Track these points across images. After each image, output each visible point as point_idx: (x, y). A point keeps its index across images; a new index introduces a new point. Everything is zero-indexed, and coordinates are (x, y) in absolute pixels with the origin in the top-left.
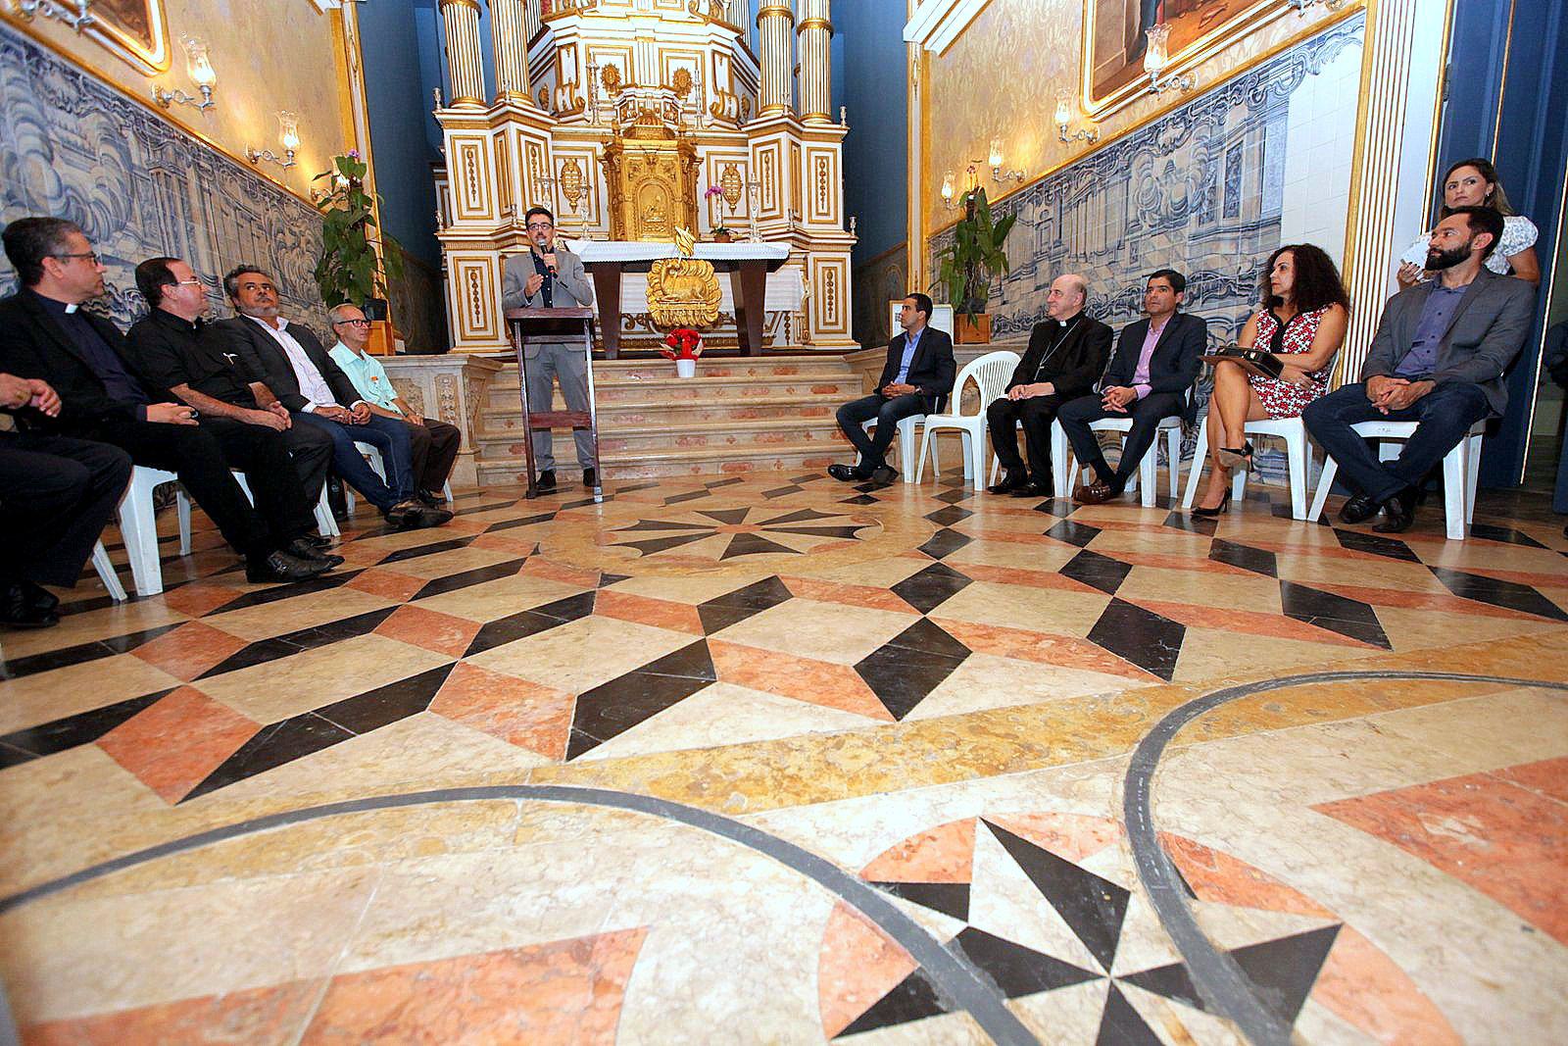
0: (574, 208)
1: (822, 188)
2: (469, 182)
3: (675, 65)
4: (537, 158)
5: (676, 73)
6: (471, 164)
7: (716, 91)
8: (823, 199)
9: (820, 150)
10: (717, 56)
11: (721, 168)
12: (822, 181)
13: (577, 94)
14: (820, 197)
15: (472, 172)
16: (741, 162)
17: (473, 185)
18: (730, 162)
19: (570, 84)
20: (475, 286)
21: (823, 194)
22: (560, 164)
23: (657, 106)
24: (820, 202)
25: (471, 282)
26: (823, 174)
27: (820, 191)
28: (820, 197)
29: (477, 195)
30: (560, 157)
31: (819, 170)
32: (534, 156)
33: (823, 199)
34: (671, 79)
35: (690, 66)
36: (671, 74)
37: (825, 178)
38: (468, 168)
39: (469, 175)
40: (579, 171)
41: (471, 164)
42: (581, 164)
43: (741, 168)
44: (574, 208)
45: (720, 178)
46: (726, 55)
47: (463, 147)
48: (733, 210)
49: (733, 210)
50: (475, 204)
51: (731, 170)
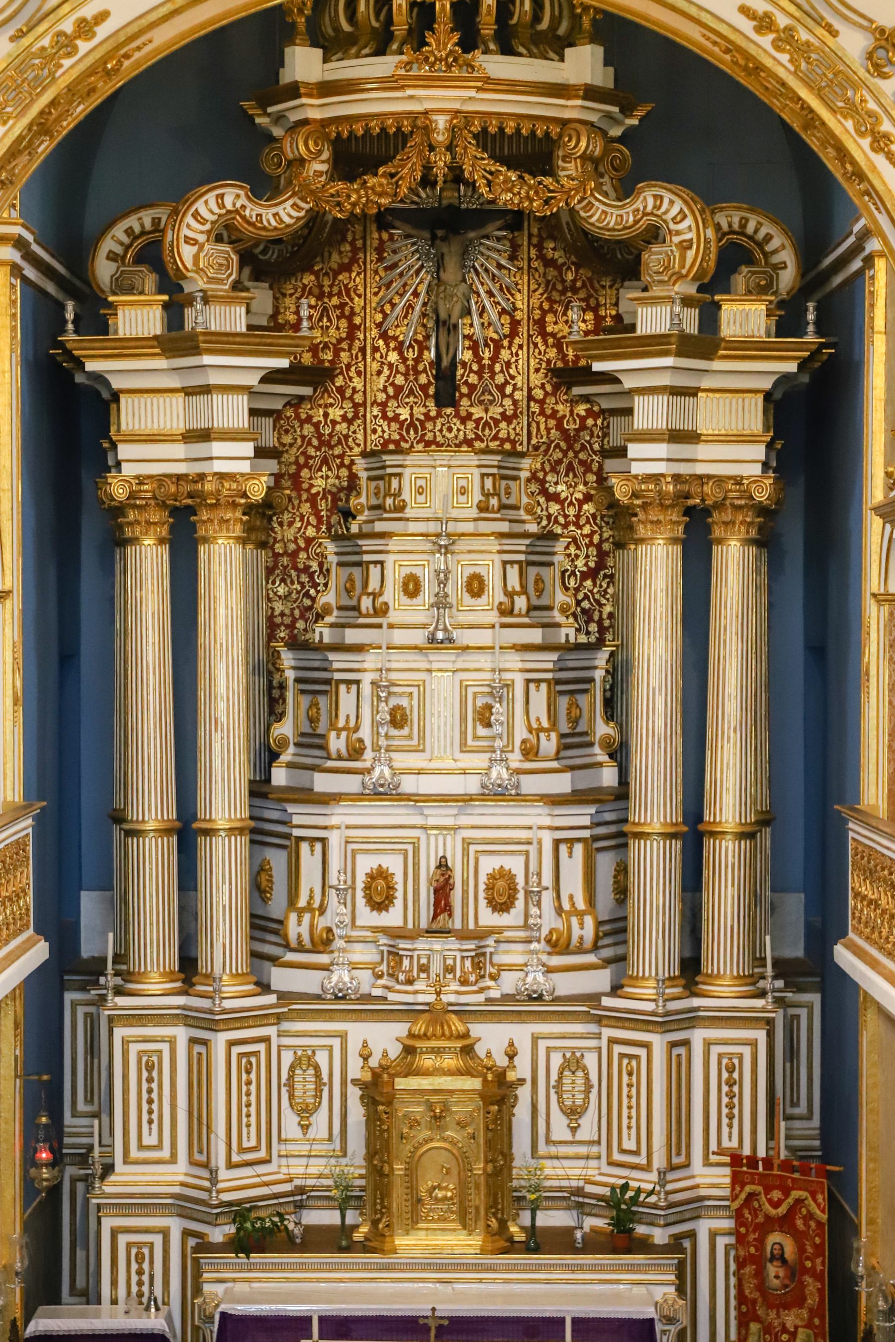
0: (305, 1128)
1: (731, 1106)
2: (145, 1107)
3: (488, 865)
4: (253, 1076)
5: (492, 877)
6: (150, 1080)
7: (559, 910)
8: (730, 1126)
9: (725, 1043)
10: (563, 848)
11: (557, 1060)
12: (731, 1095)
13: (322, 923)
14: (725, 1121)
15: (150, 1091)
16: (589, 1049)
17: (150, 1112)
18: (573, 1050)
19: (309, 908)
20: (140, 1272)
21: (731, 1117)
22: (288, 1058)
23: (450, 962)
24: (725, 1130)
25: (134, 1266)
26: (731, 1083)
27: (725, 1111)
28: (725, 1121)
29: (155, 1126)
30: (288, 1047)
31: (725, 1075)
32: (248, 1072)
33: (730, 1126)
34: (482, 887)
35: (515, 865)
36: (483, 878)
37: (736, 1089)
38: (145, 1086)
39: (145, 1096)
40: (317, 1068)
41: (150, 1080)
42: (322, 1058)
43: (590, 1061)
44: (305, 1128)
45: (554, 1077)
46: (579, 840)
47: (140, 1054)
48: (574, 1130)
49: (574, 1130)
50: (147, 1141)
51: (573, 1064)
